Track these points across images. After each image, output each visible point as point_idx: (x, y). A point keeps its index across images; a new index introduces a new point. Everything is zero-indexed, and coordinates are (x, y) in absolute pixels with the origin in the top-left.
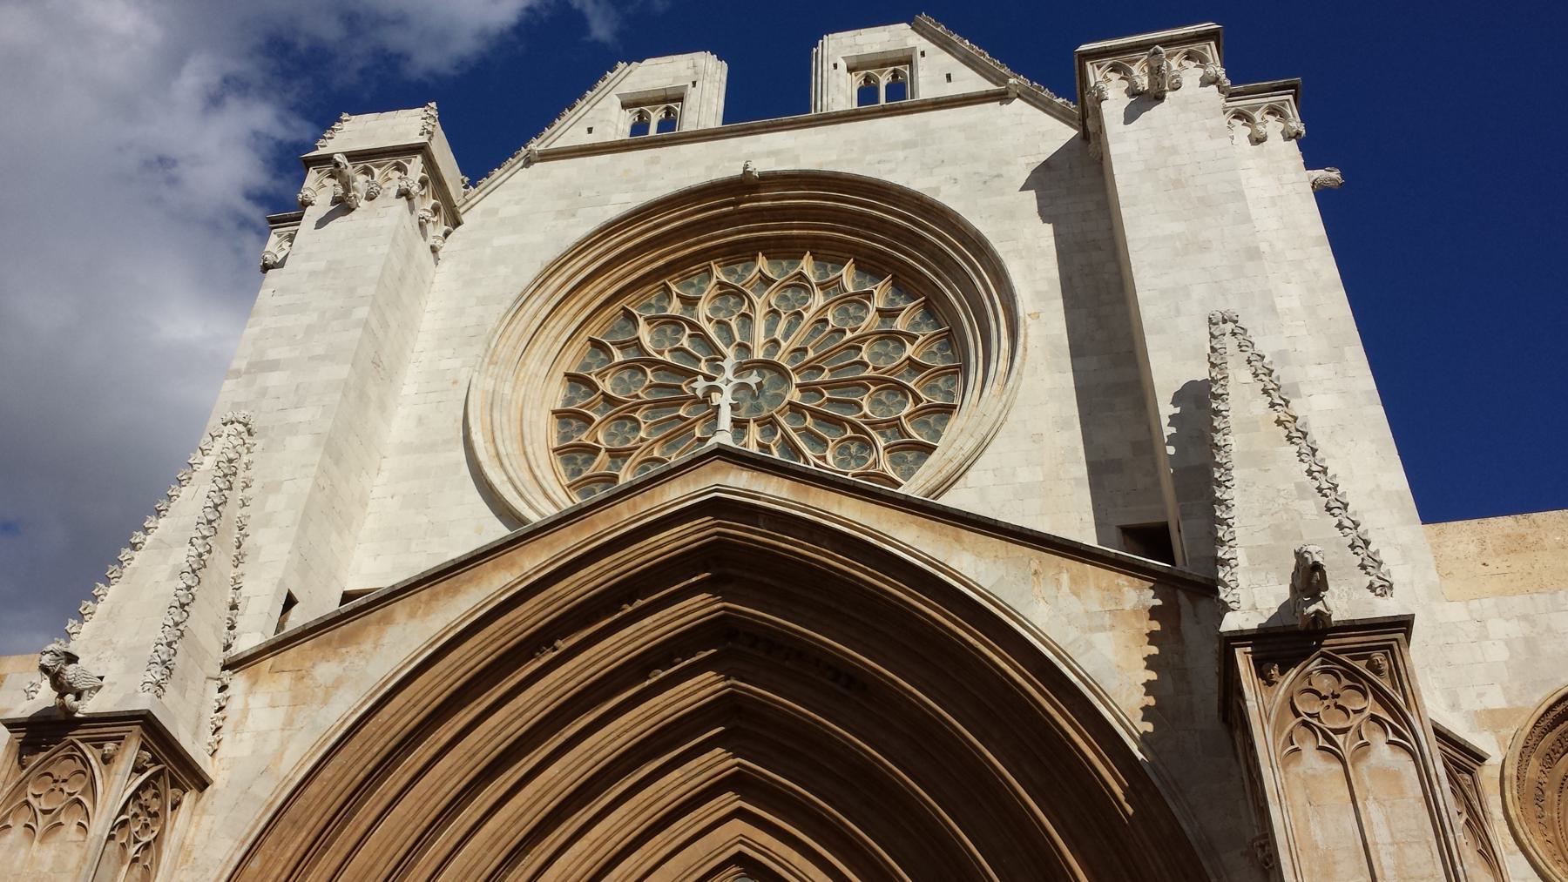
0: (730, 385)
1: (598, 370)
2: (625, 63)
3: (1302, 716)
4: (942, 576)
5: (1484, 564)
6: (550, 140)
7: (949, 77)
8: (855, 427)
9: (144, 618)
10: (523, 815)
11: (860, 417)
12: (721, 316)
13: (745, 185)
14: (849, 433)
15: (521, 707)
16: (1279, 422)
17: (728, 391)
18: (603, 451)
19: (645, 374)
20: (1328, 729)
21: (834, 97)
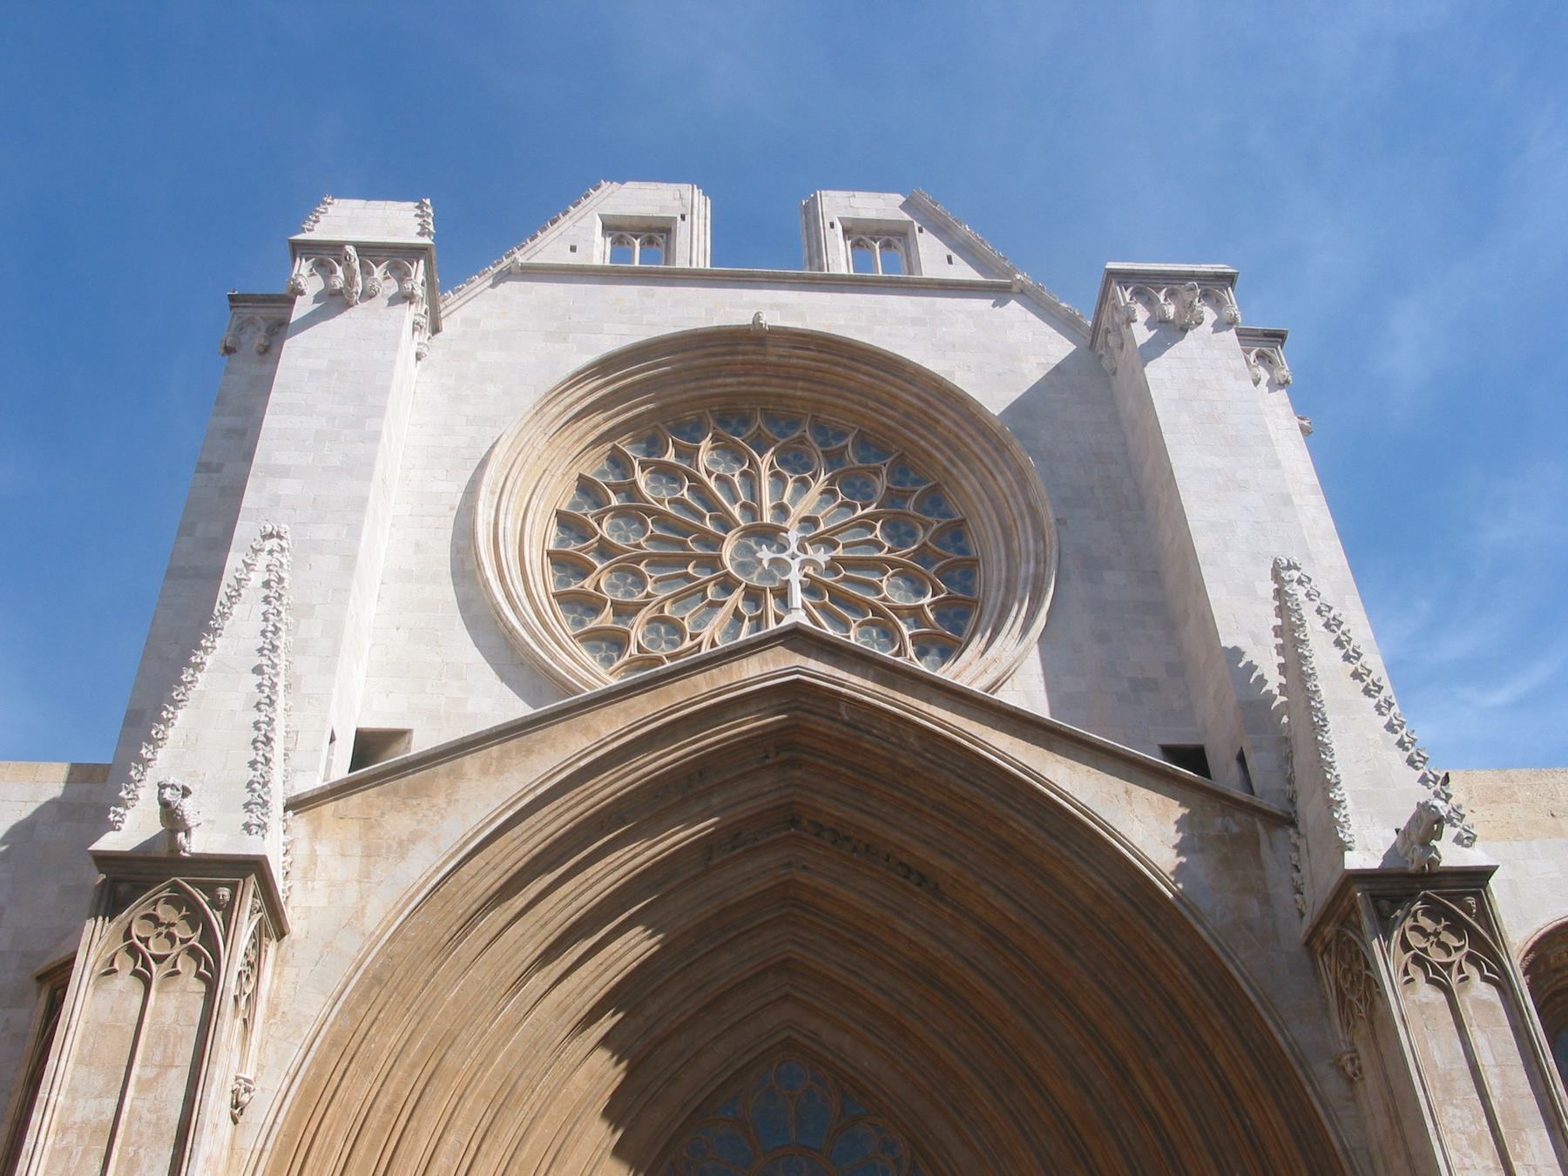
0: (798, 560)
1: (593, 512)
2: (608, 183)
3: (1413, 949)
4: (1039, 786)
5: (1472, 811)
6: (532, 252)
7: (950, 260)
8: (876, 611)
9: (228, 750)
10: (586, 988)
11: (880, 600)
12: (720, 470)
13: (751, 338)
14: (870, 616)
15: (590, 878)
16: (1356, 675)
17: (795, 565)
18: (609, 603)
19: (643, 523)
20: (1438, 963)
21: (834, 258)
